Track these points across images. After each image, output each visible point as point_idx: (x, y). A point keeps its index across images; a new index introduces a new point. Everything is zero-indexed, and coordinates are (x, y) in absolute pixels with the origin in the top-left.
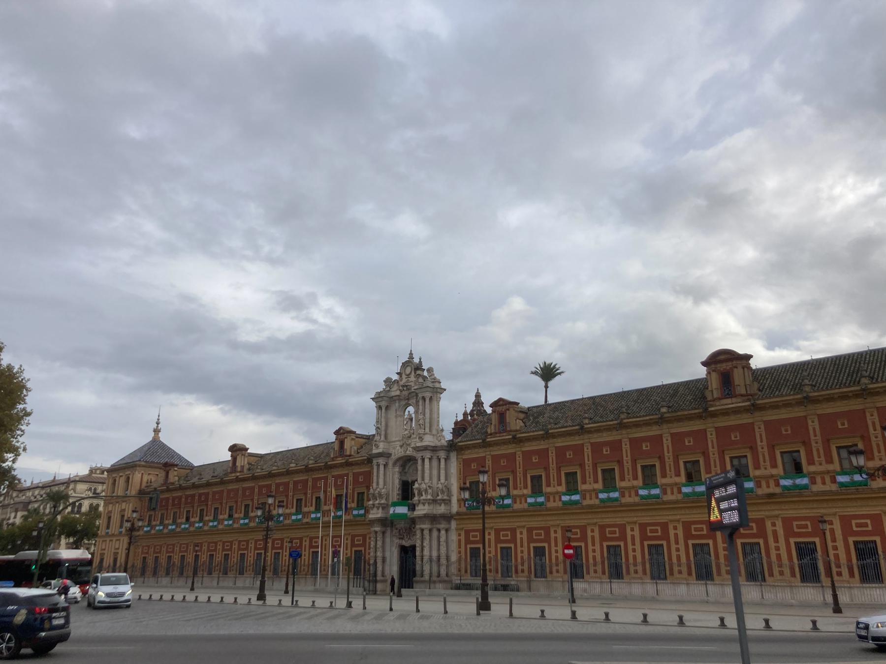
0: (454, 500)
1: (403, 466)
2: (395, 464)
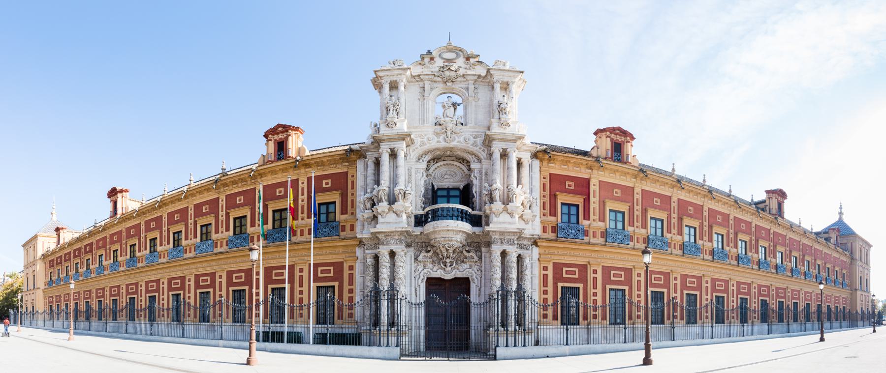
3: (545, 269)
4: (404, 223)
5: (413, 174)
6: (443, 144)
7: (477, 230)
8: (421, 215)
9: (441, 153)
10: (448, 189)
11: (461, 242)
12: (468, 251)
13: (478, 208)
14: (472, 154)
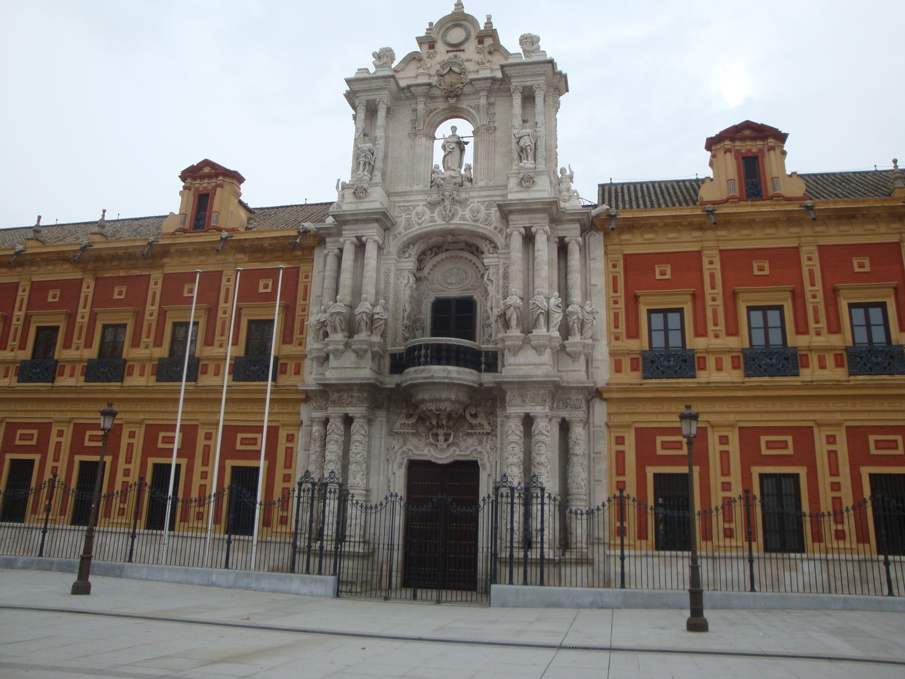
0: (602, 352)
1: (421, 261)
2: (404, 249)
3: (620, 441)
6: (440, 223)
7: (488, 378)
8: (401, 354)
9: (440, 239)
11: (458, 401)
12: (474, 416)
14: (485, 238)
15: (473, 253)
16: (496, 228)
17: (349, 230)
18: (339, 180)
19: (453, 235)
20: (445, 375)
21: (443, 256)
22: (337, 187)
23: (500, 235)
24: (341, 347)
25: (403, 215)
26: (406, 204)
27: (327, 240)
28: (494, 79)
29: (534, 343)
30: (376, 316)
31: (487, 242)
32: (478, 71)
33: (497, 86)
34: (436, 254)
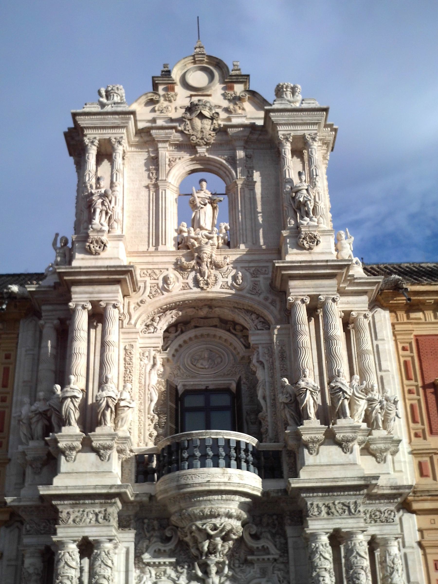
4: (113, 473)
5: (136, 360)
7: (275, 485)
10: (206, 392)
13: (270, 433)
15: (229, 331)
16: (266, 299)
17: (81, 293)
18: (57, 235)
19: (210, 307)
20: (226, 480)
21: (191, 333)
22: (54, 244)
23: (272, 307)
24: (78, 444)
25: (148, 279)
26: (151, 267)
27: (44, 308)
28: (253, 127)
29: (339, 436)
30: (122, 404)
31: (254, 316)
32: (229, 119)
33: (255, 136)
34: (182, 332)
